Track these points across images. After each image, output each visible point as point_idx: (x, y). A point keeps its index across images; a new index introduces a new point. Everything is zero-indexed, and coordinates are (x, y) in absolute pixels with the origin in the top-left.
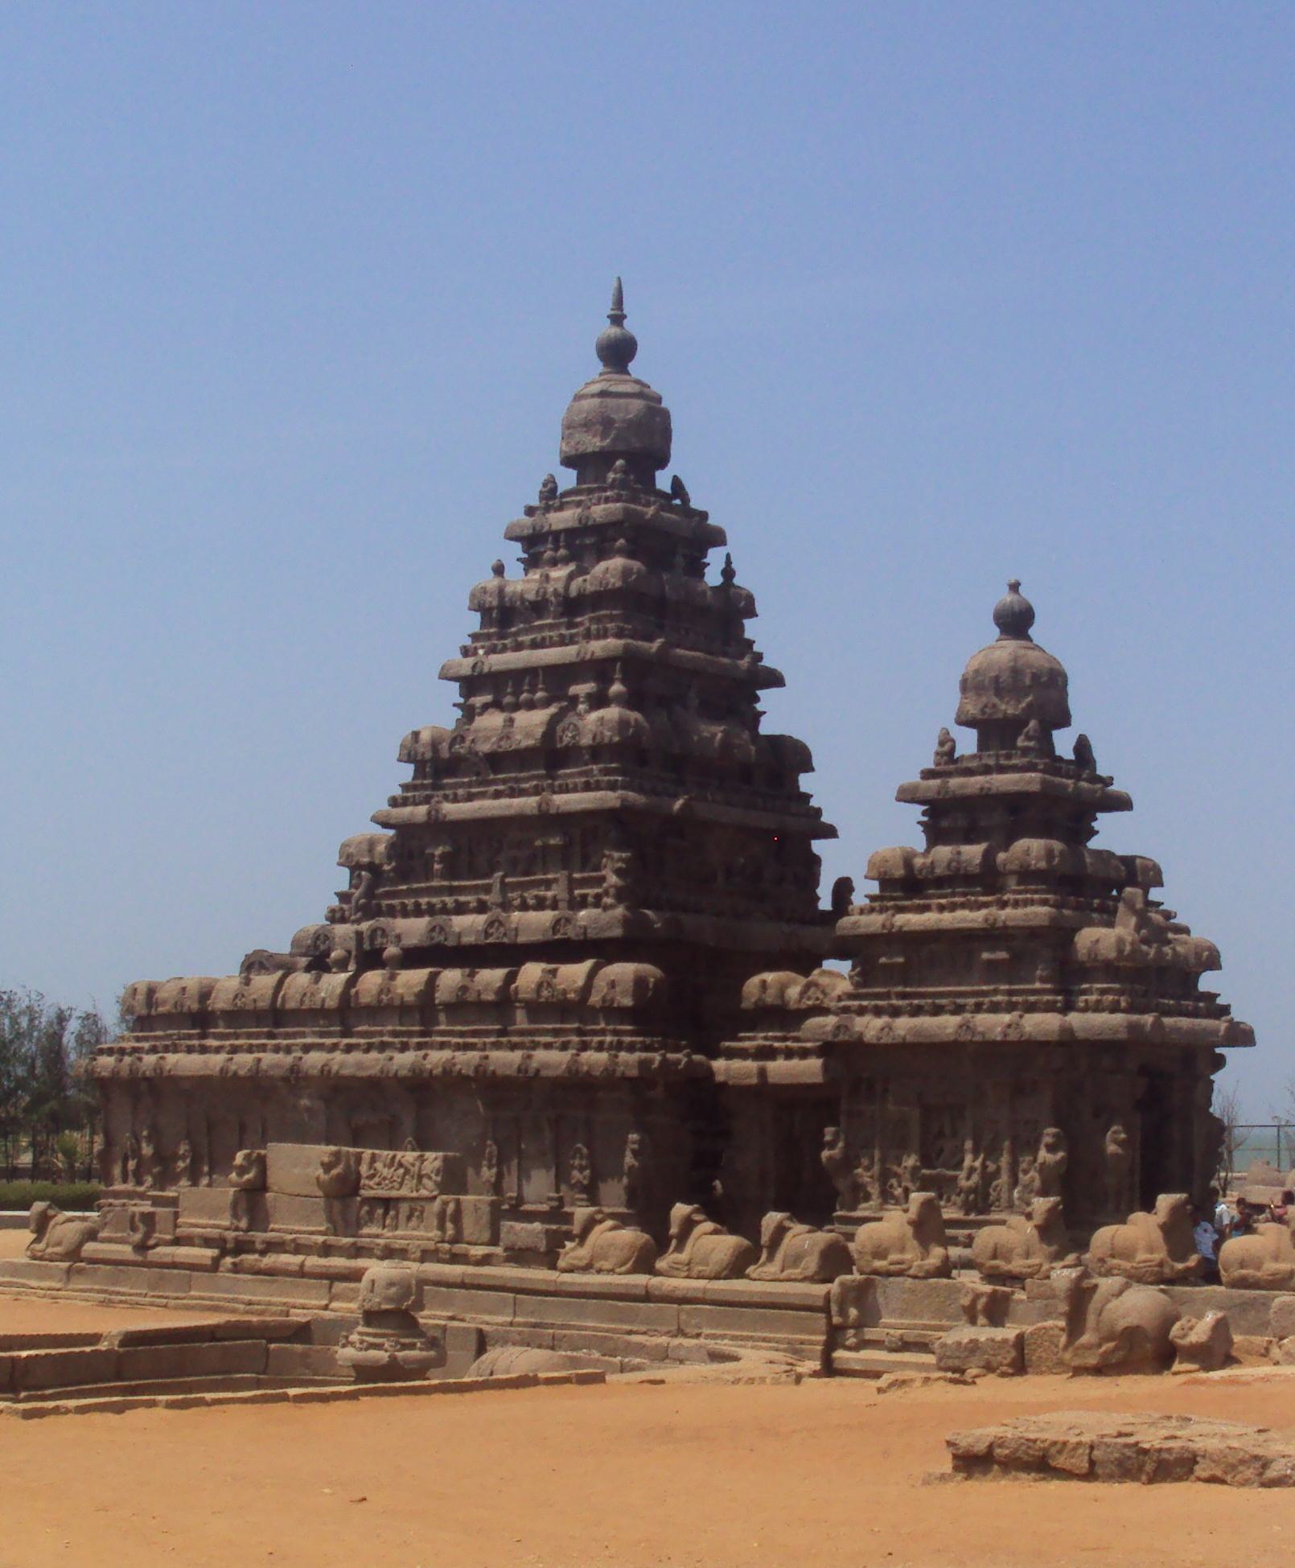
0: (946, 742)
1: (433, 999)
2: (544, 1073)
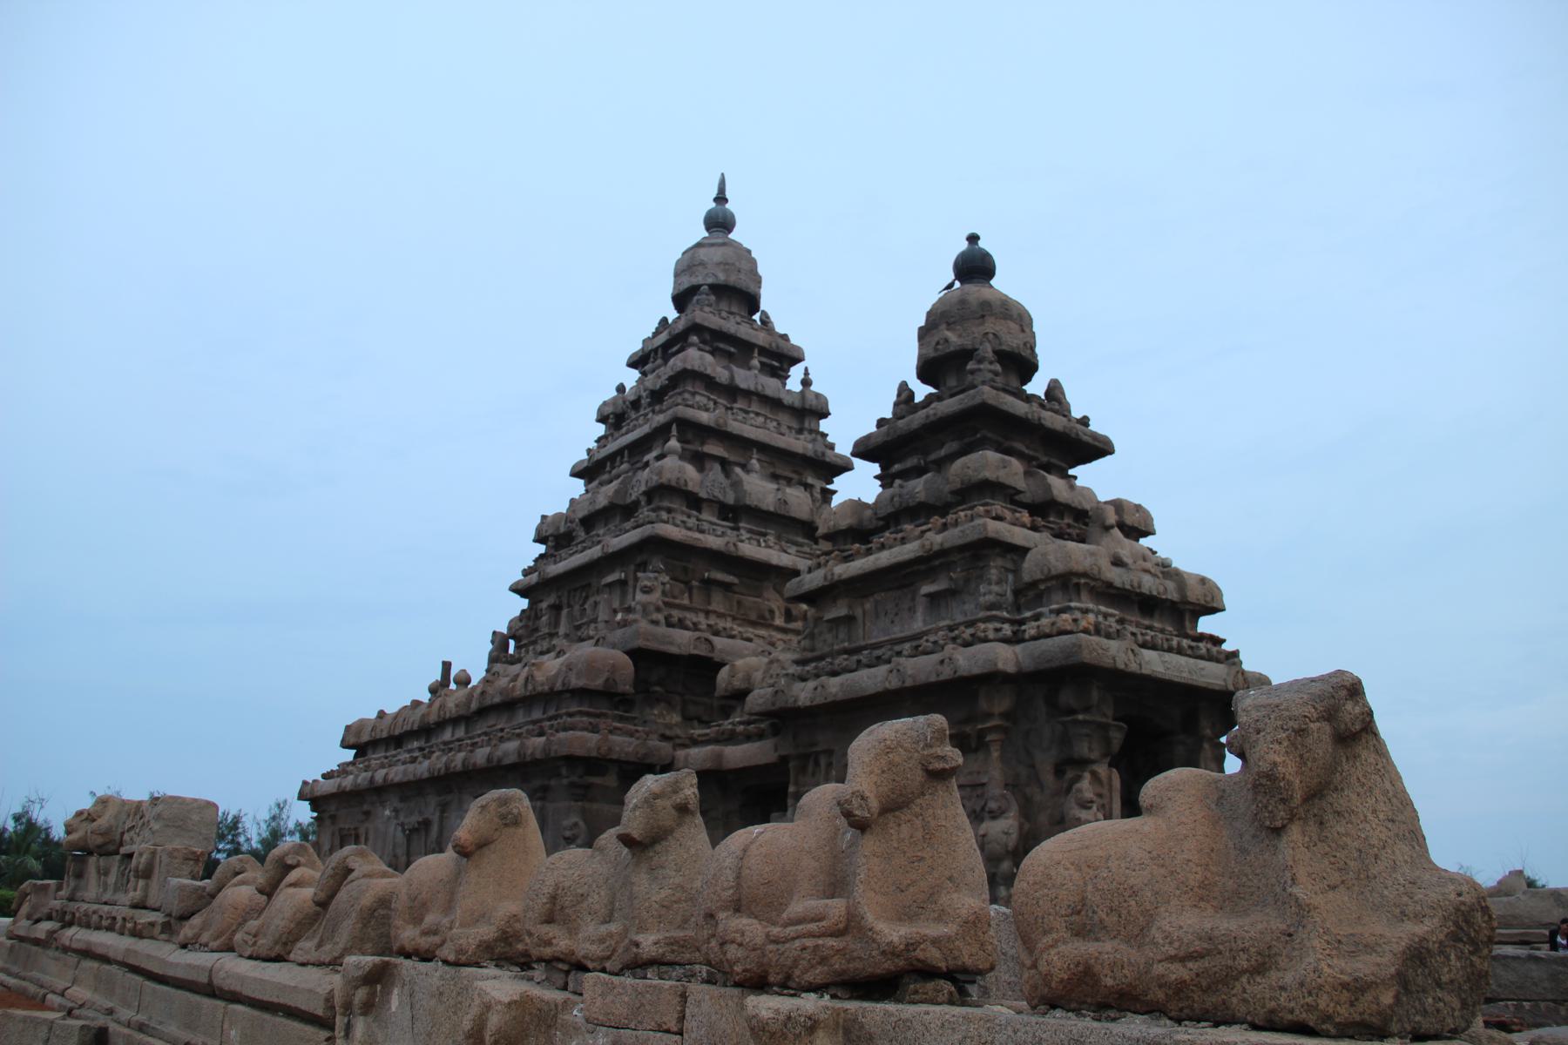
0: (905, 394)
1: (469, 707)
2: (507, 761)
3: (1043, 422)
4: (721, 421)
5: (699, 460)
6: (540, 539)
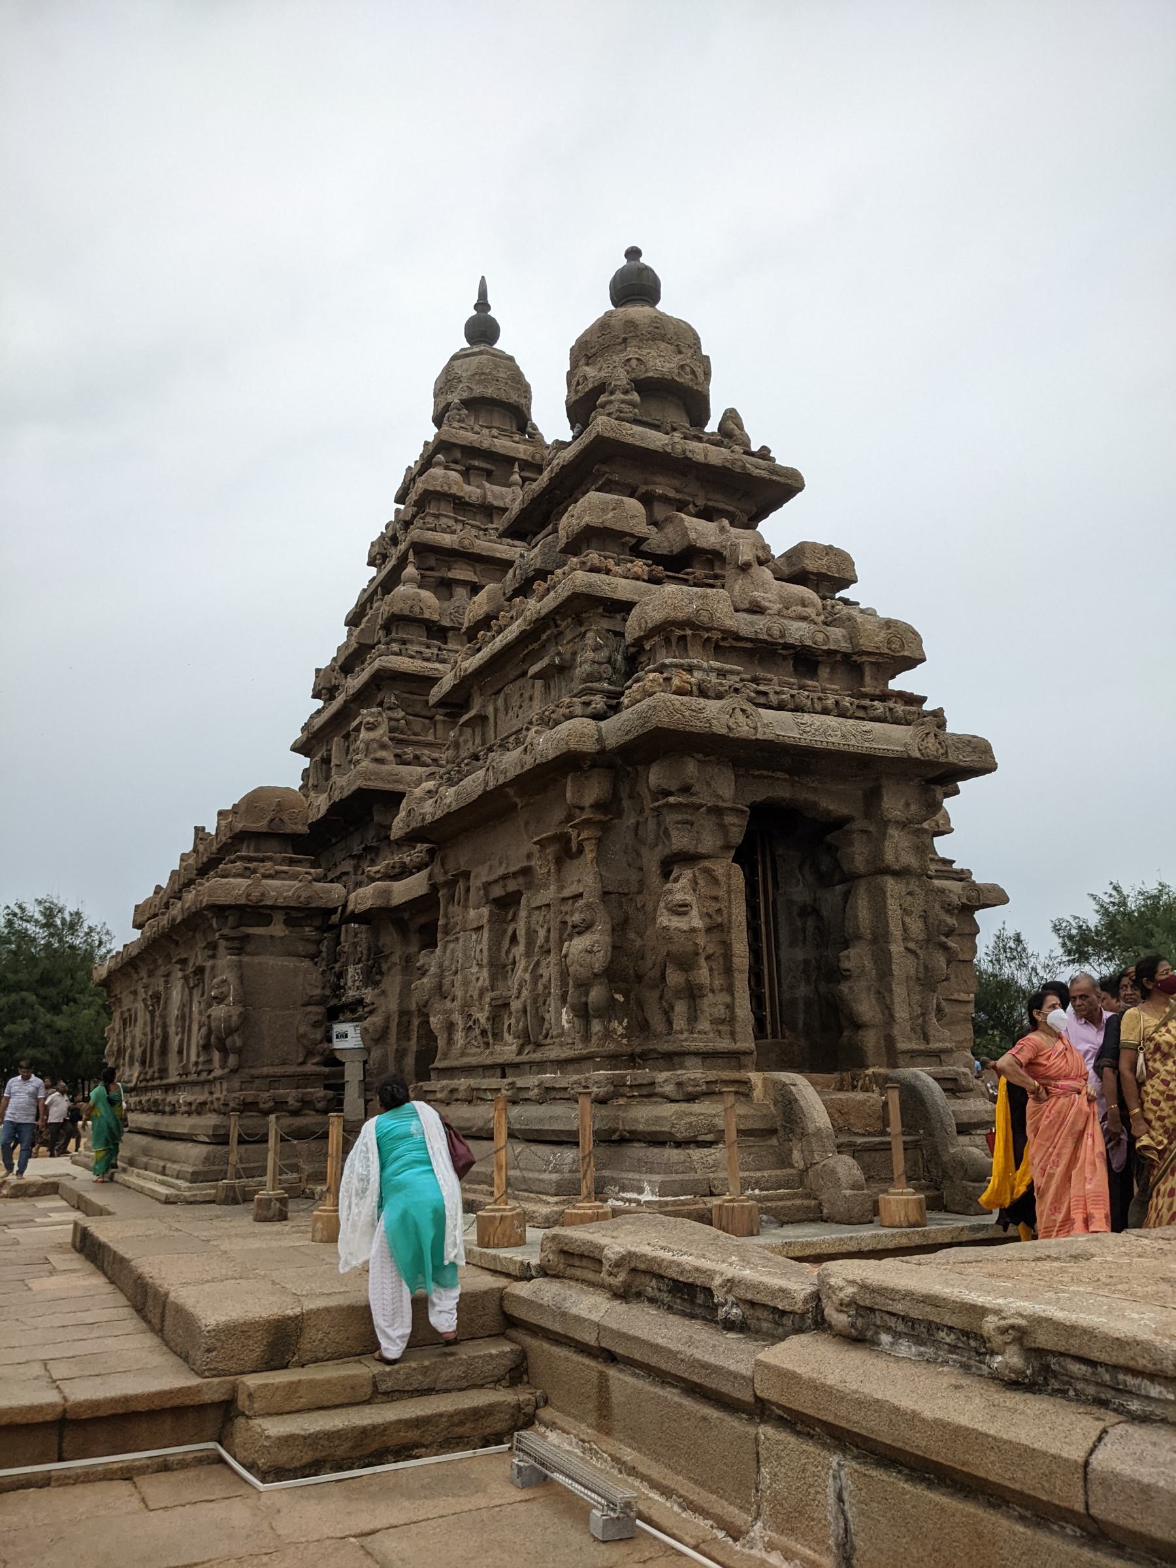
3: (690, 455)
4: (466, 542)
5: (445, 587)
6: (316, 695)
